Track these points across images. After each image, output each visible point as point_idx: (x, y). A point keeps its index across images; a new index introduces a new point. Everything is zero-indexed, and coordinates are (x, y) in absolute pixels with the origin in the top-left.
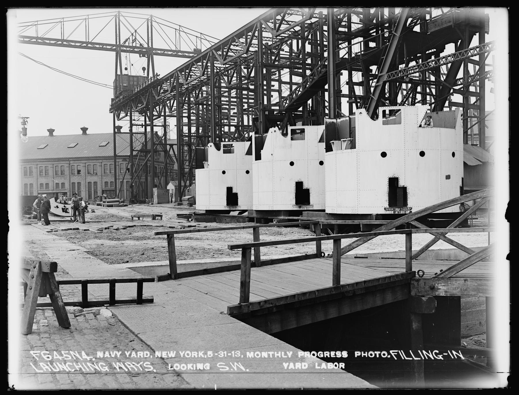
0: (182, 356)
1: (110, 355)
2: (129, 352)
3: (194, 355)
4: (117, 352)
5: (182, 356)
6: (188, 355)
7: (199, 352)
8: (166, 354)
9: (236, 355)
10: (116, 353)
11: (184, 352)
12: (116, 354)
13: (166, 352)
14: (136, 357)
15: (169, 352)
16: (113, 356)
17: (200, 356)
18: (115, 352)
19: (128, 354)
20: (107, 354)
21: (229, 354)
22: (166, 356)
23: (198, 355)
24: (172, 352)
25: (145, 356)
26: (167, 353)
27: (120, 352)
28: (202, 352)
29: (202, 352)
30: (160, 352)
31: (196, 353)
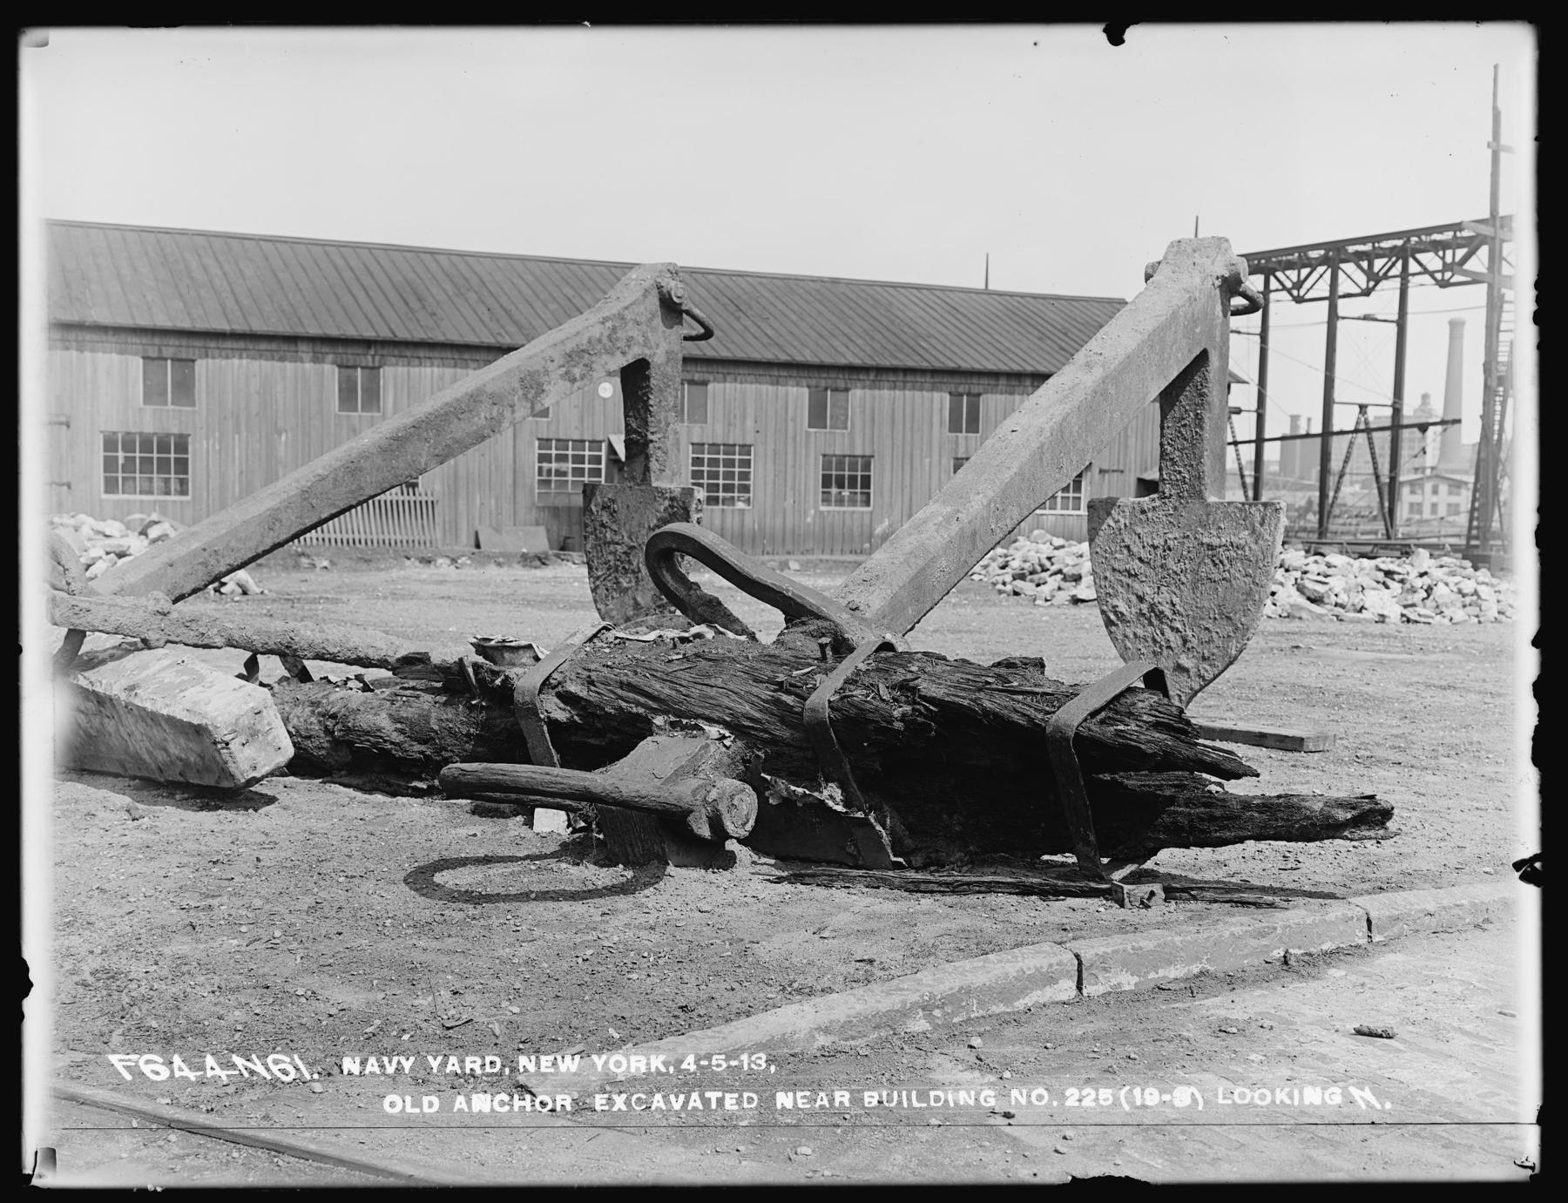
0: (600, 1069)
1: (382, 1066)
2: (440, 1058)
3: (638, 1064)
4: (402, 1059)
5: (600, 1069)
6: (618, 1064)
7: (653, 1057)
8: (550, 1064)
9: (753, 1066)
10: (399, 1063)
11: (604, 1057)
12: (399, 1069)
13: (551, 1058)
14: (459, 1072)
15: (559, 1058)
16: (390, 1070)
17: (653, 1070)
18: (395, 1059)
19: (435, 1064)
20: (372, 1066)
21: (734, 1063)
22: (552, 1070)
23: (648, 1064)
24: (568, 1058)
25: (488, 1069)
26: (554, 1064)
27: (412, 1059)
28: (662, 1058)
29: (662, 1058)
30: (533, 1058)
31: (644, 1060)
